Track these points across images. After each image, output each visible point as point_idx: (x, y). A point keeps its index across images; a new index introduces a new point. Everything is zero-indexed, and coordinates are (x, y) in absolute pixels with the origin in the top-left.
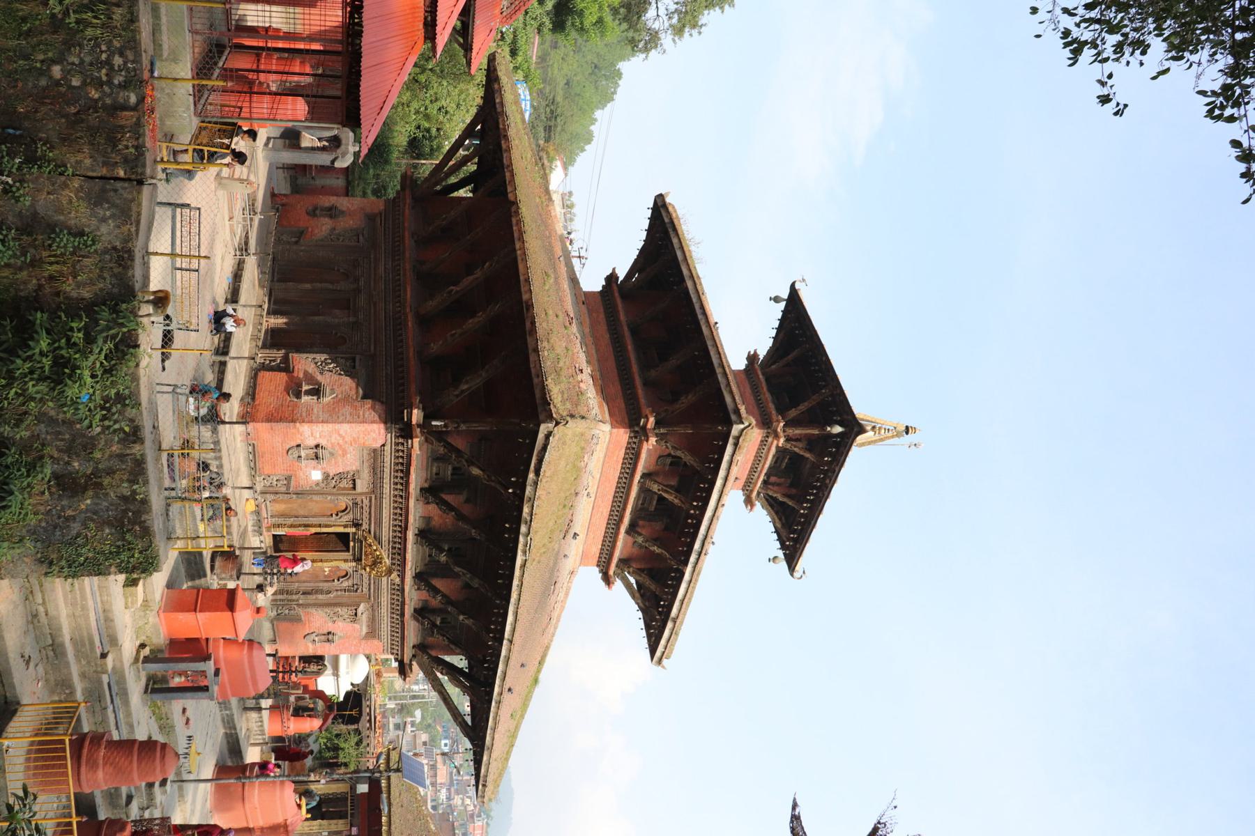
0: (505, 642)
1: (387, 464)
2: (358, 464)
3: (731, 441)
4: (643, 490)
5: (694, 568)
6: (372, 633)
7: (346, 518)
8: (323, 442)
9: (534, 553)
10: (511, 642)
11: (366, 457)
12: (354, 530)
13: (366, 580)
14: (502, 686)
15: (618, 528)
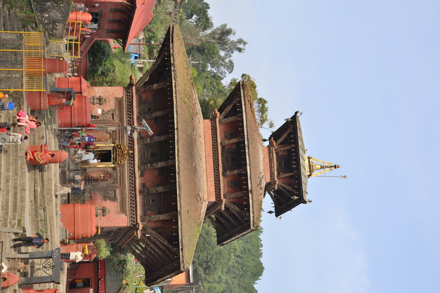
0: (176, 131)
1: (124, 106)
2: (114, 106)
3: (241, 87)
4: (223, 147)
5: (249, 155)
6: (123, 209)
7: (110, 141)
8: (102, 95)
9: (178, 79)
10: (177, 129)
11: (117, 104)
12: (113, 145)
13: (119, 175)
14: (178, 160)
15: (219, 175)
